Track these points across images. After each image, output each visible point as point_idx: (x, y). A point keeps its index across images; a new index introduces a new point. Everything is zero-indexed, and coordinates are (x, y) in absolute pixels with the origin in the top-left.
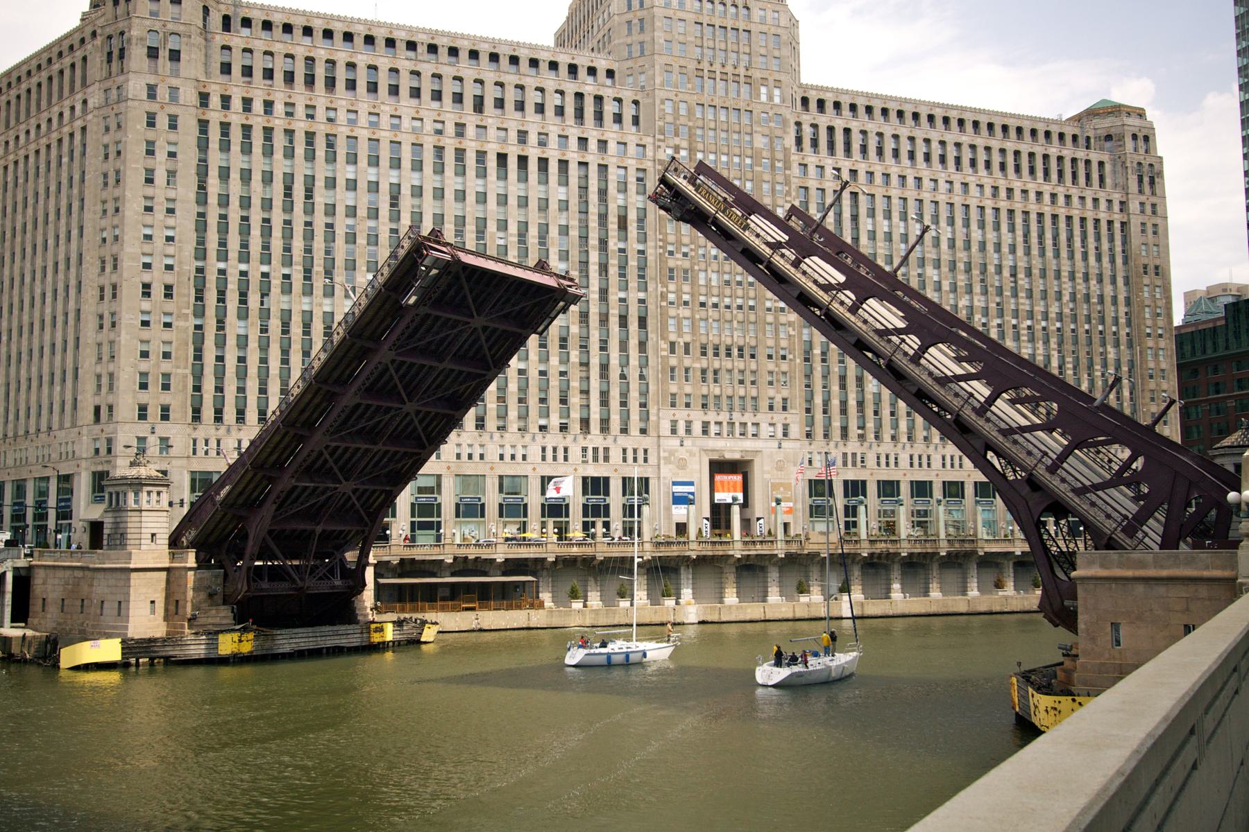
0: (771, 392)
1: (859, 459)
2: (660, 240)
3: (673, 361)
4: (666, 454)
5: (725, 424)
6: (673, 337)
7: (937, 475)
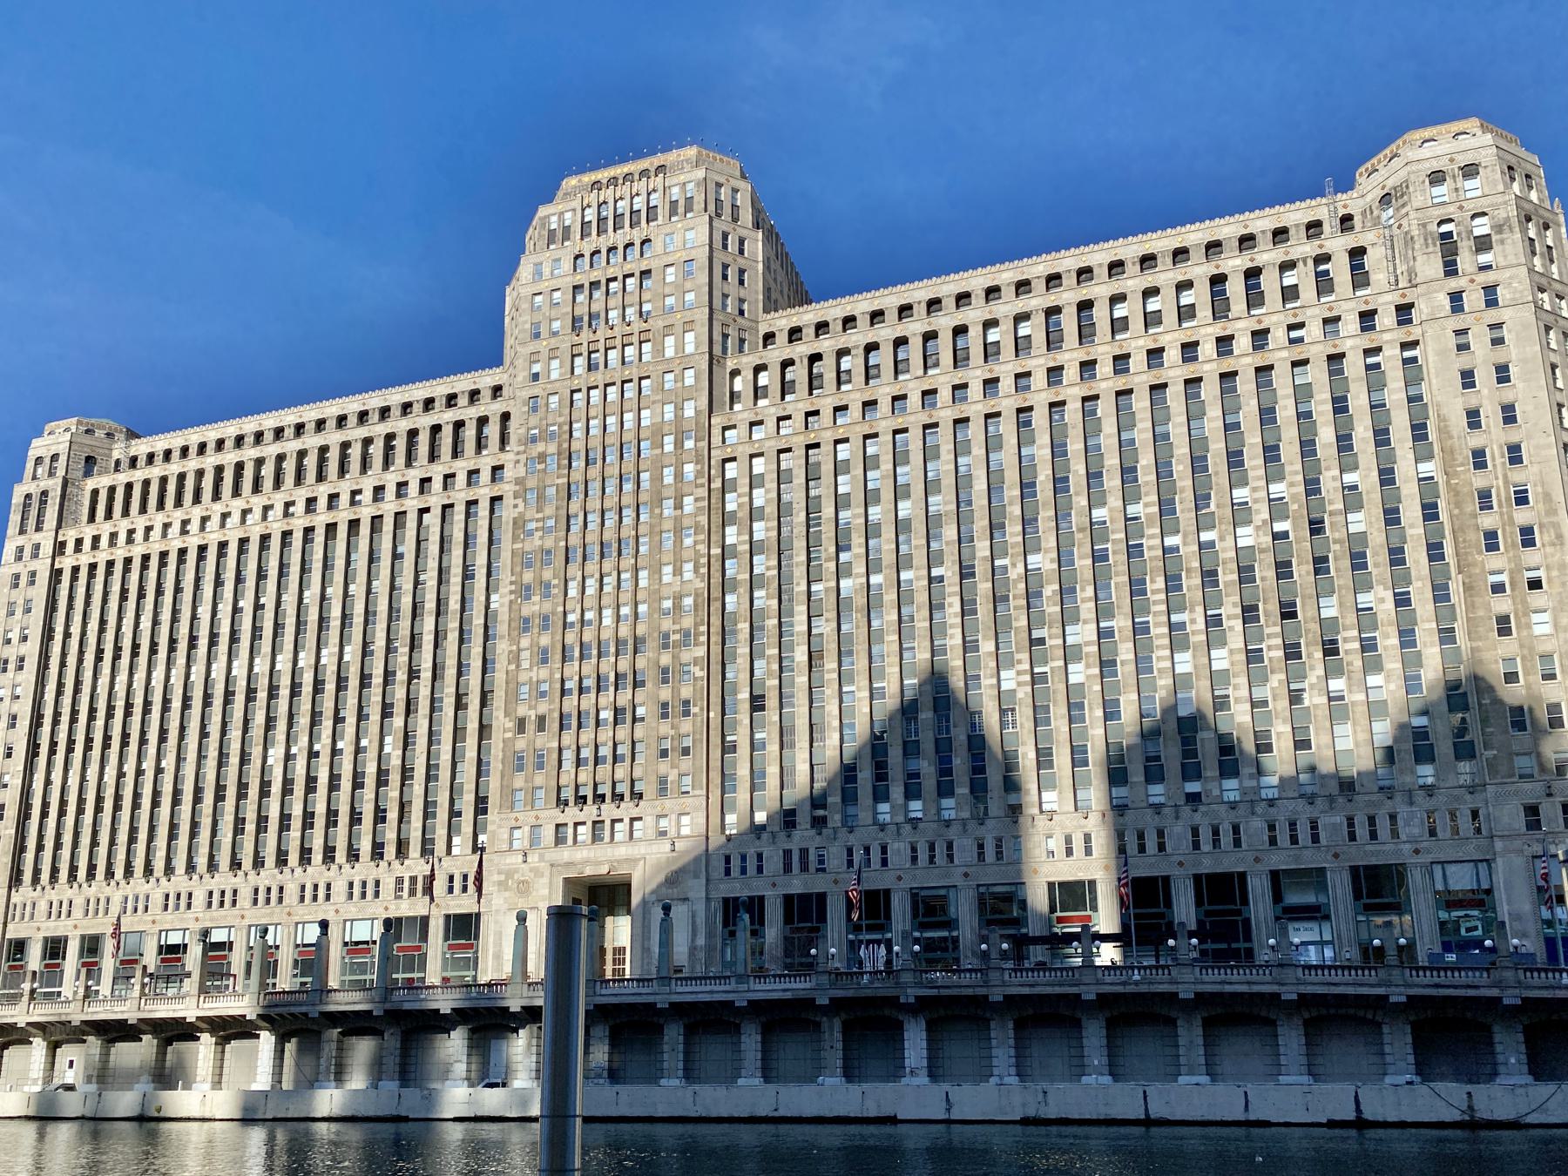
0: (663, 767)
1: (812, 857)
2: (512, 583)
3: (521, 744)
4: (502, 877)
5: (589, 824)
6: (522, 711)
7: (966, 875)
